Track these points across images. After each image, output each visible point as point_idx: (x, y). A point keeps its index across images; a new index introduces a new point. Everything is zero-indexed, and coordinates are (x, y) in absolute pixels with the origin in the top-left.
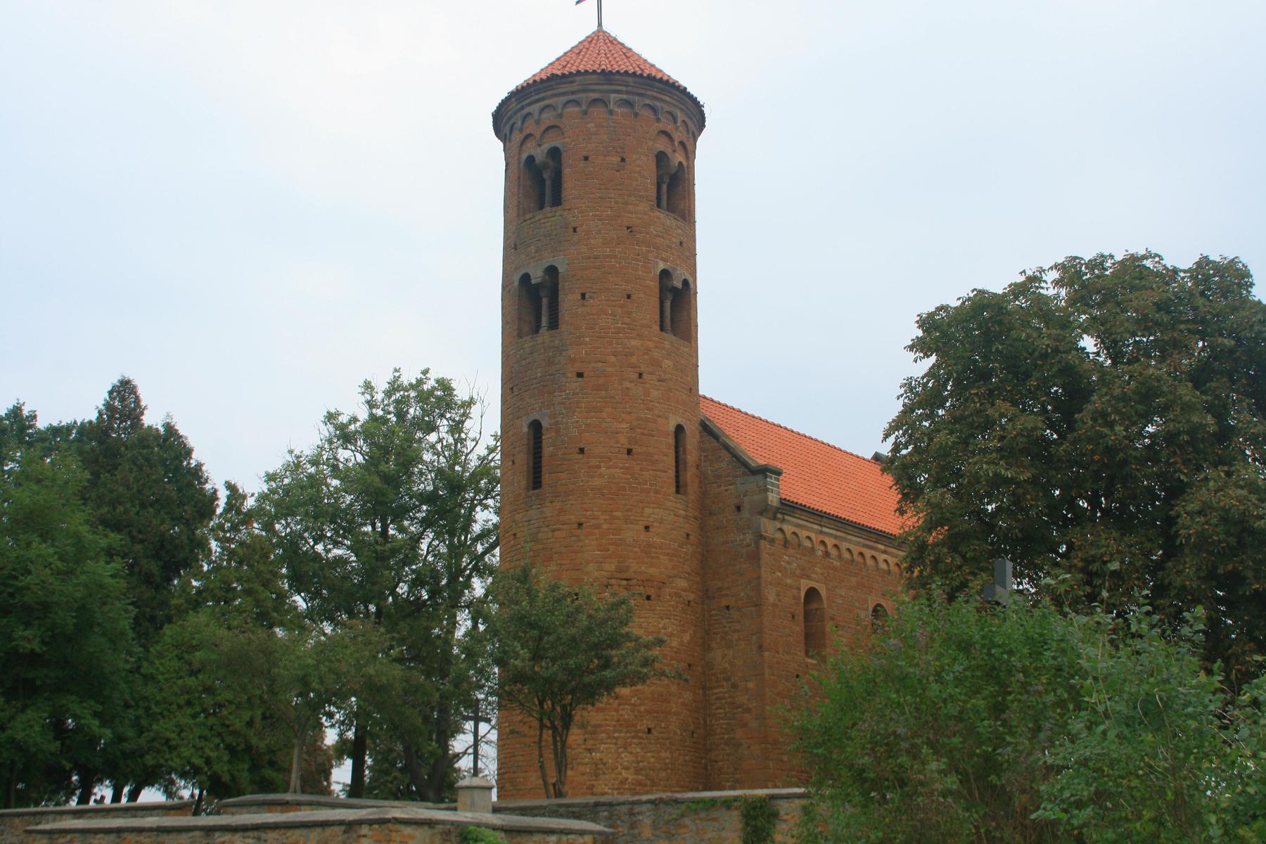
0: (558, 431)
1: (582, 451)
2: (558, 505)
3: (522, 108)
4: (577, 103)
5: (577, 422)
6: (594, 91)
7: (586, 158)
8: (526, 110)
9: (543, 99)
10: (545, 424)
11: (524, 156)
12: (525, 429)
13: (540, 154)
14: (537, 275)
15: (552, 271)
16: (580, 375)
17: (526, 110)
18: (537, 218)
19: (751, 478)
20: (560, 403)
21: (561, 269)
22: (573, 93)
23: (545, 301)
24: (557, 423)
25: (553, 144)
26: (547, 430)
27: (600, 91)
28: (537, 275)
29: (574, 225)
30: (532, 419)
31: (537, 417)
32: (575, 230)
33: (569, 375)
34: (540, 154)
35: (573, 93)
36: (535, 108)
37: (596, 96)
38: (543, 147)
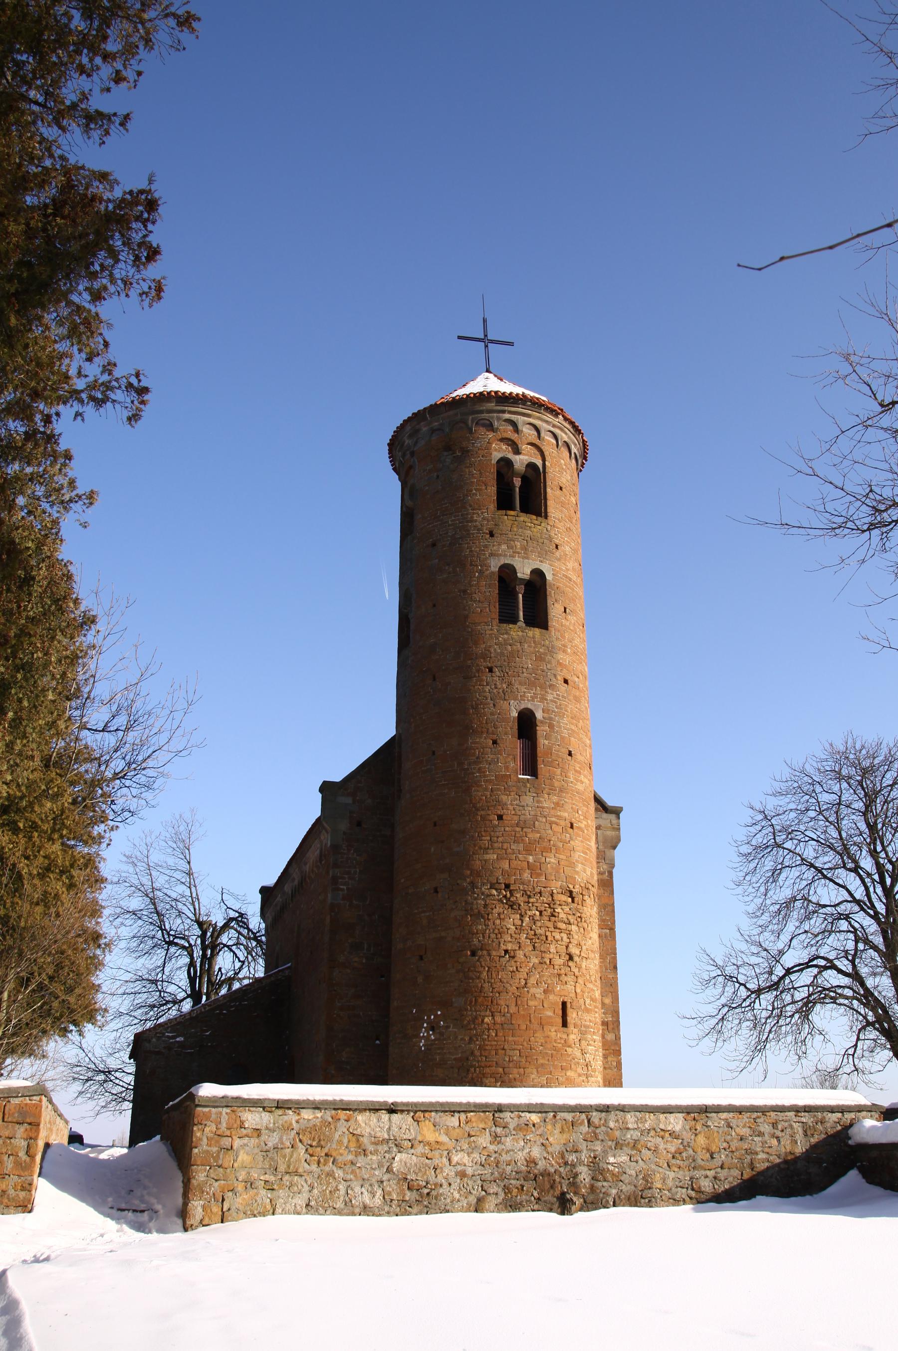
0: (551, 726)
1: (570, 754)
2: (555, 799)
3: (504, 412)
4: (555, 437)
5: (567, 724)
6: (566, 434)
7: (561, 489)
8: (507, 416)
9: (529, 416)
10: (539, 715)
11: (496, 456)
12: (515, 714)
13: (520, 461)
14: (524, 571)
15: (538, 574)
16: (566, 681)
17: (507, 416)
18: (522, 519)
19: (605, 815)
20: (552, 701)
21: (549, 577)
22: (554, 426)
23: (520, 596)
24: (550, 719)
25: (534, 460)
26: (542, 722)
27: (569, 437)
28: (524, 571)
29: (557, 542)
30: (523, 707)
31: (530, 706)
32: (557, 547)
33: (559, 678)
34: (520, 461)
35: (554, 426)
36: (520, 419)
37: (566, 440)
38: (521, 457)
